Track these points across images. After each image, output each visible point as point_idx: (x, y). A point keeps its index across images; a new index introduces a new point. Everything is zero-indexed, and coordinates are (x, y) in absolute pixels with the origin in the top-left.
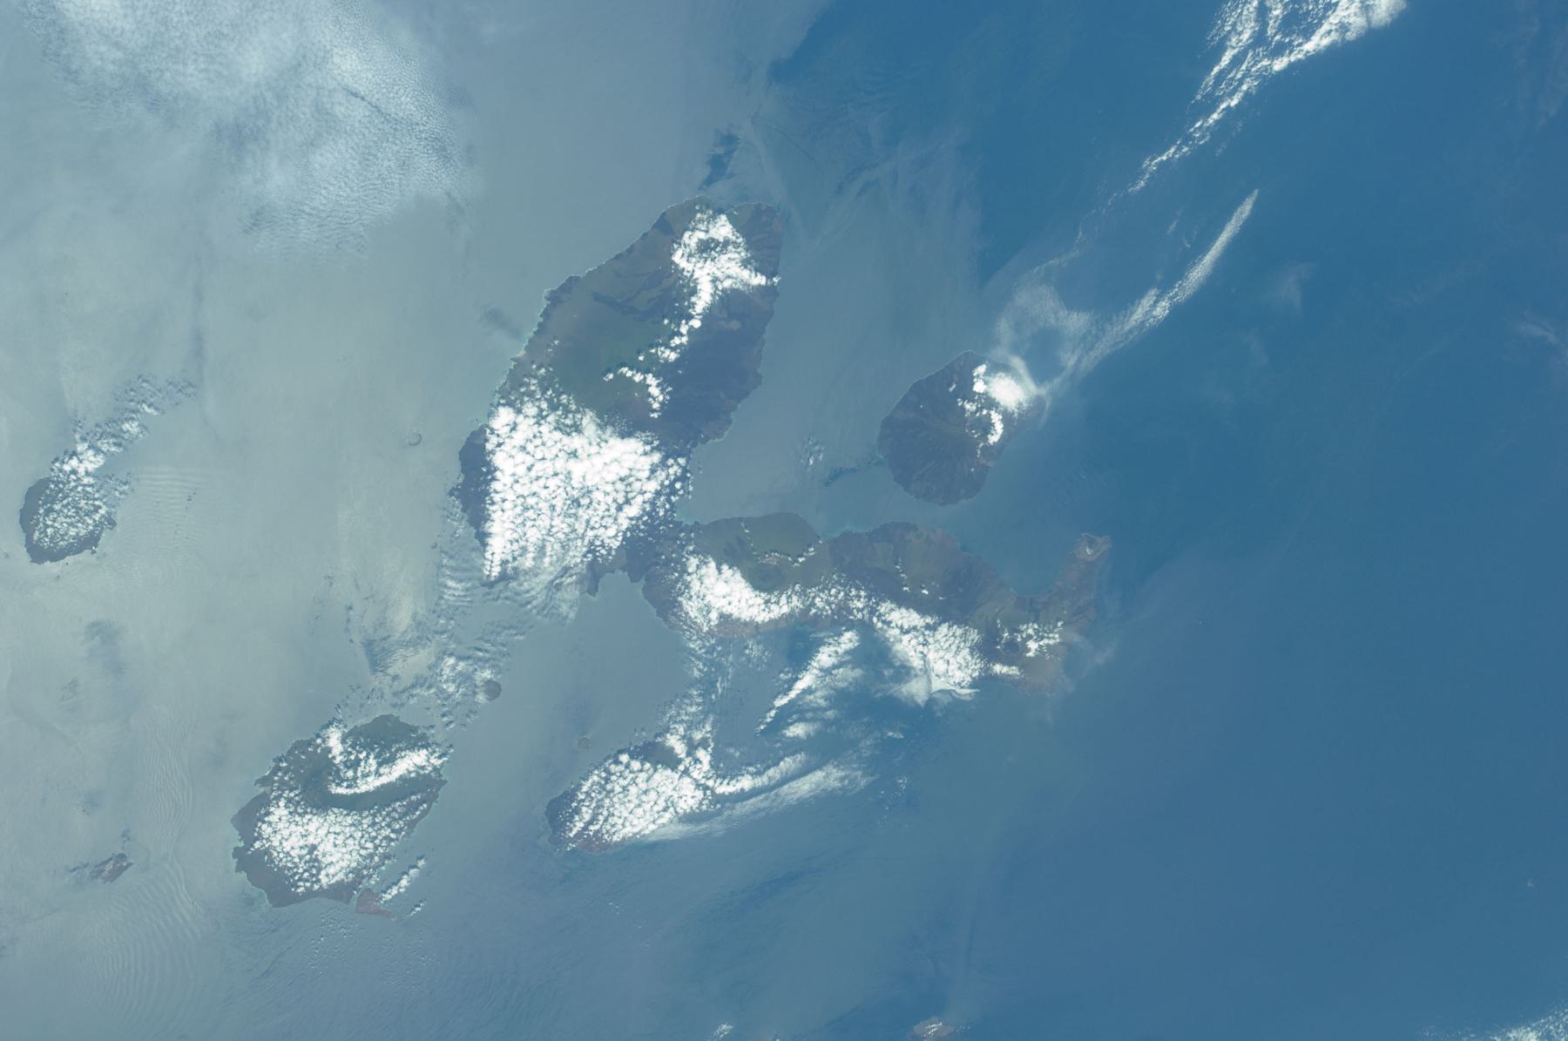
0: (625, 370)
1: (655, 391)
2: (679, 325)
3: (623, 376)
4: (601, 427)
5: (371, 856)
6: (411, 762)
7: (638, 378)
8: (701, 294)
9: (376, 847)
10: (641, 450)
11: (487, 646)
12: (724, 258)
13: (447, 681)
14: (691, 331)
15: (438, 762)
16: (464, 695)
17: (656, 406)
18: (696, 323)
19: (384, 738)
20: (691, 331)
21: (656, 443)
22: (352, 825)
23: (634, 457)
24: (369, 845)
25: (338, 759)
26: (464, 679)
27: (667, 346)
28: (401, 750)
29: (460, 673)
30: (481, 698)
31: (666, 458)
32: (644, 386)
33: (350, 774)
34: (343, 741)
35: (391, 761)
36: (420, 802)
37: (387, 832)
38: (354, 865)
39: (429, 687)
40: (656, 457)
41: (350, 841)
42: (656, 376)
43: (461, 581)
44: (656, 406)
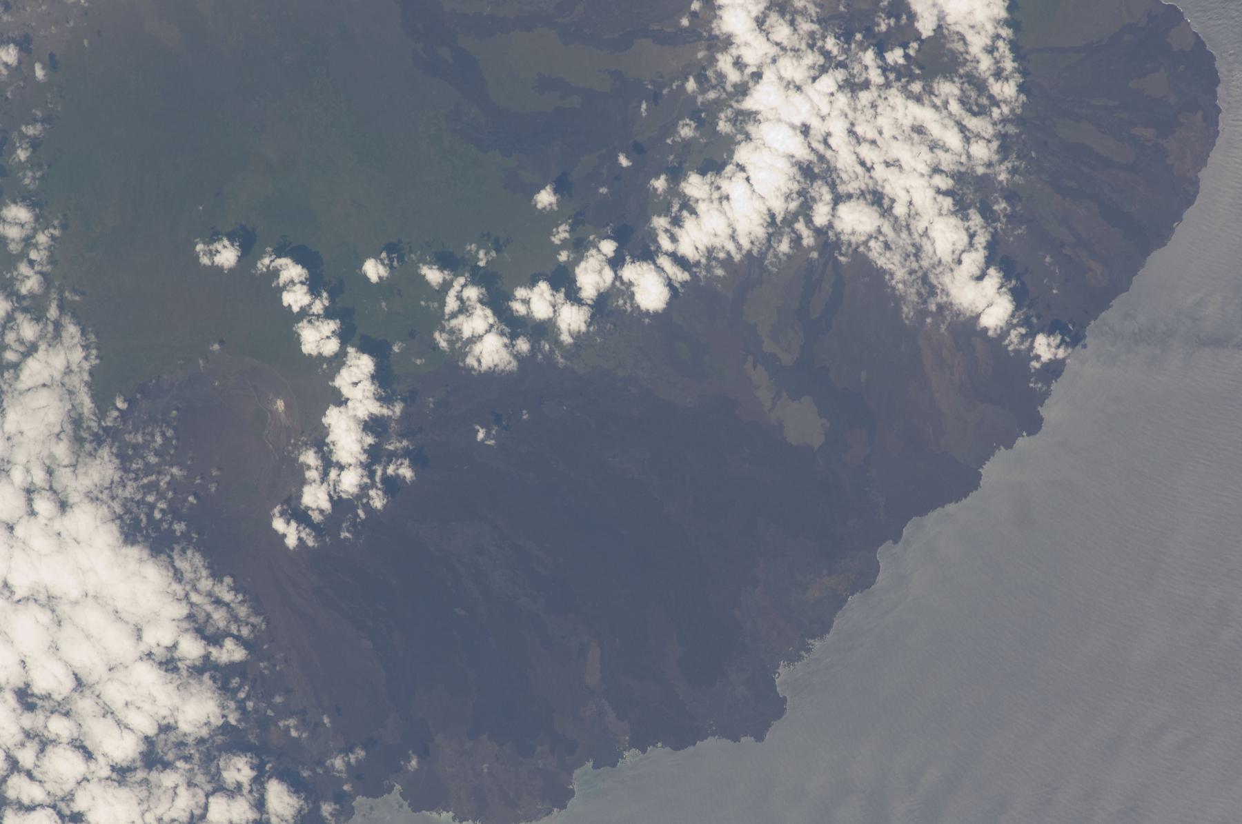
0: (292, 271)
1: (345, 433)
2: (580, 247)
3: (270, 287)
4: (83, 436)
7: (317, 338)
8: (734, 187)
10: (160, 635)
12: (902, 110)
14: (610, 307)
17: (315, 497)
18: (650, 290)
20: (610, 307)
21: (231, 652)
23: (120, 644)
27: (497, 301)
31: (226, 741)
32: (316, 386)
40: (198, 711)
42: (385, 380)
44: (315, 497)
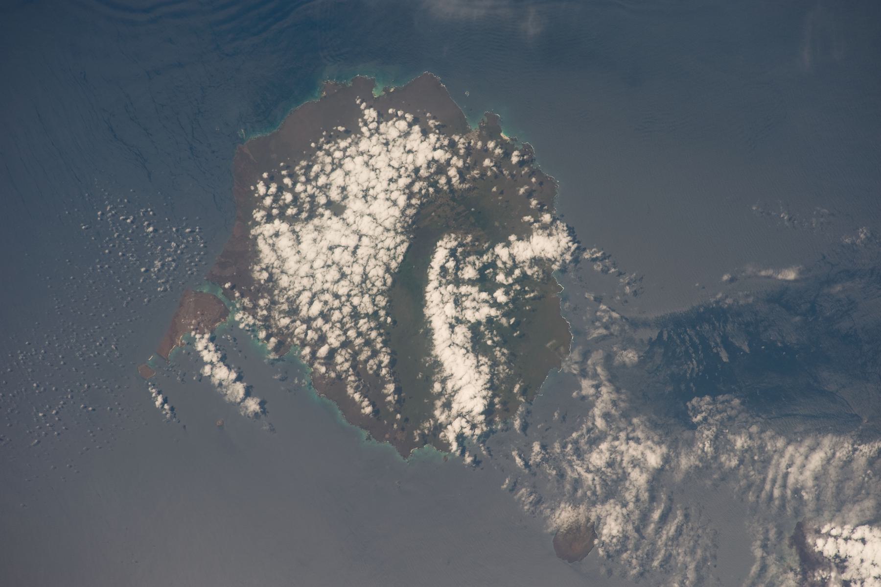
5: (293, 312)
6: (466, 383)
9: (308, 321)
11: (671, 529)
13: (613, 450)
15: (450, 435)
16: (578, 482)
19: (523, 338)
22: (365, 277)
24: (317, 307)
25: (501, 251)
26: (613, 486)
28: (494, 364)
29: (625, 476)
30: (564, 516)
33: (469, 273)
34: (536, 261)
35: (477, 345)
36: (377, 400)
37: (334, 339)
38: (284, 281)
39: (606, 416)
41: (333, 274)
43: (816, 478)
